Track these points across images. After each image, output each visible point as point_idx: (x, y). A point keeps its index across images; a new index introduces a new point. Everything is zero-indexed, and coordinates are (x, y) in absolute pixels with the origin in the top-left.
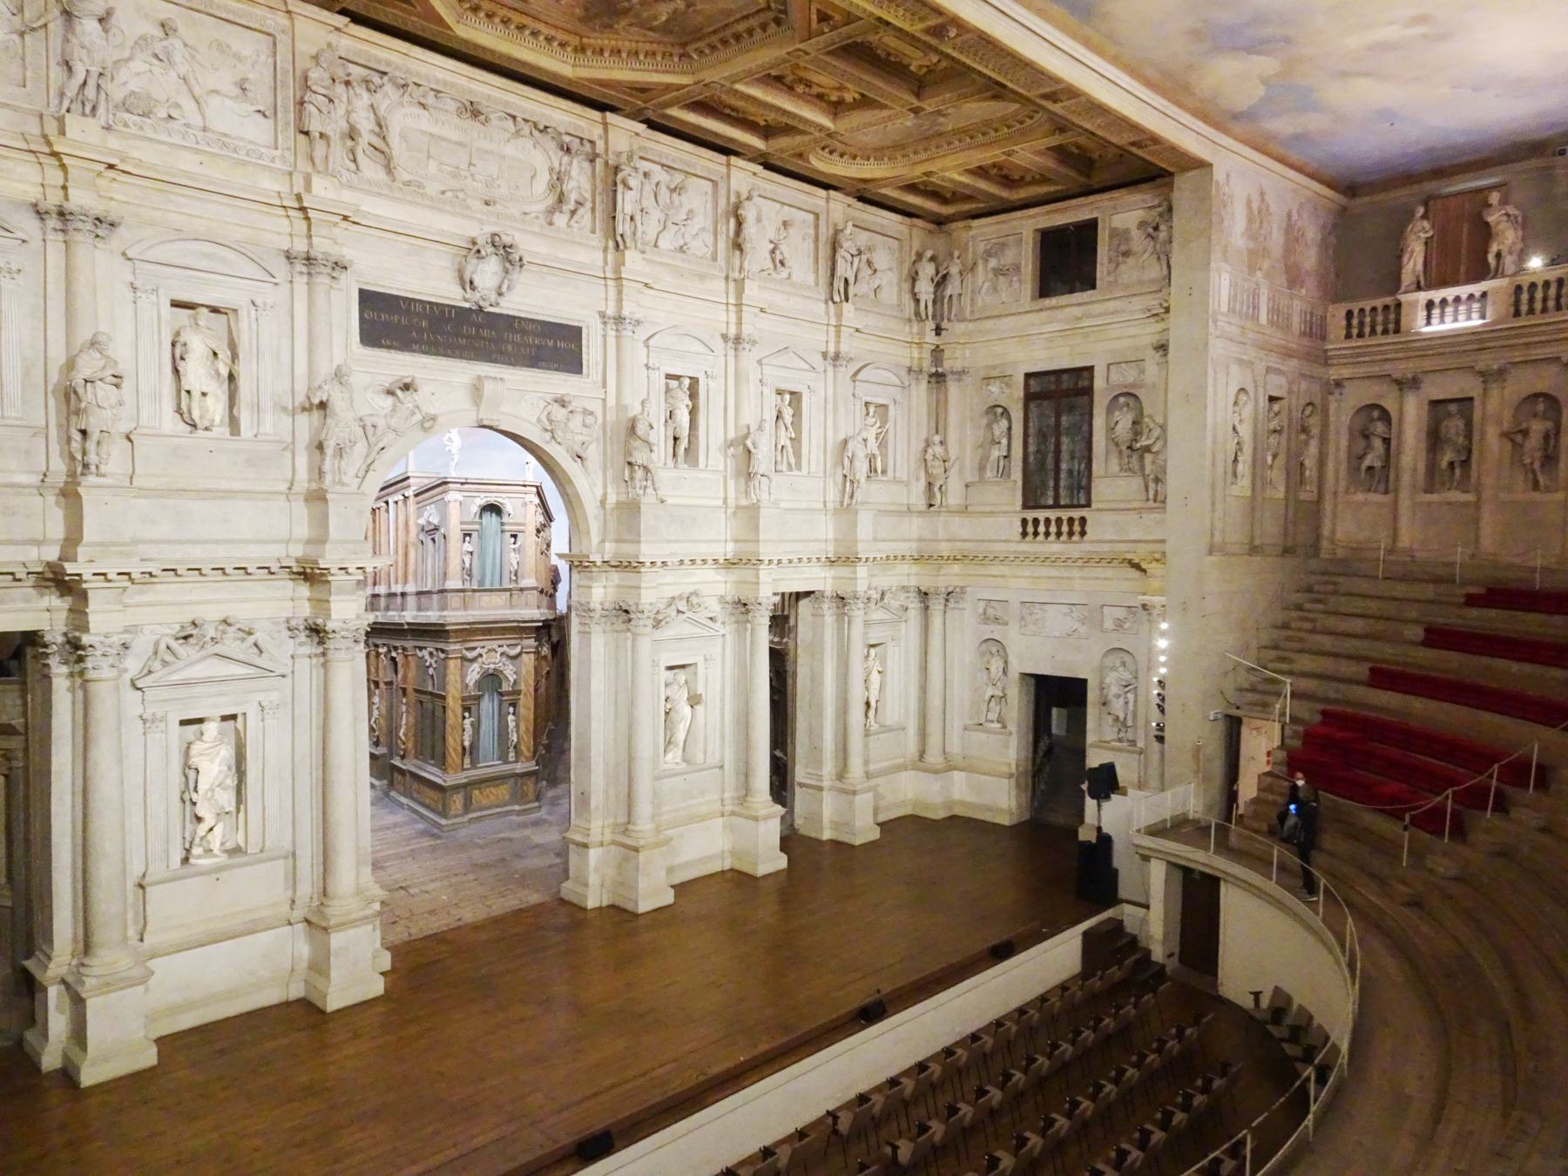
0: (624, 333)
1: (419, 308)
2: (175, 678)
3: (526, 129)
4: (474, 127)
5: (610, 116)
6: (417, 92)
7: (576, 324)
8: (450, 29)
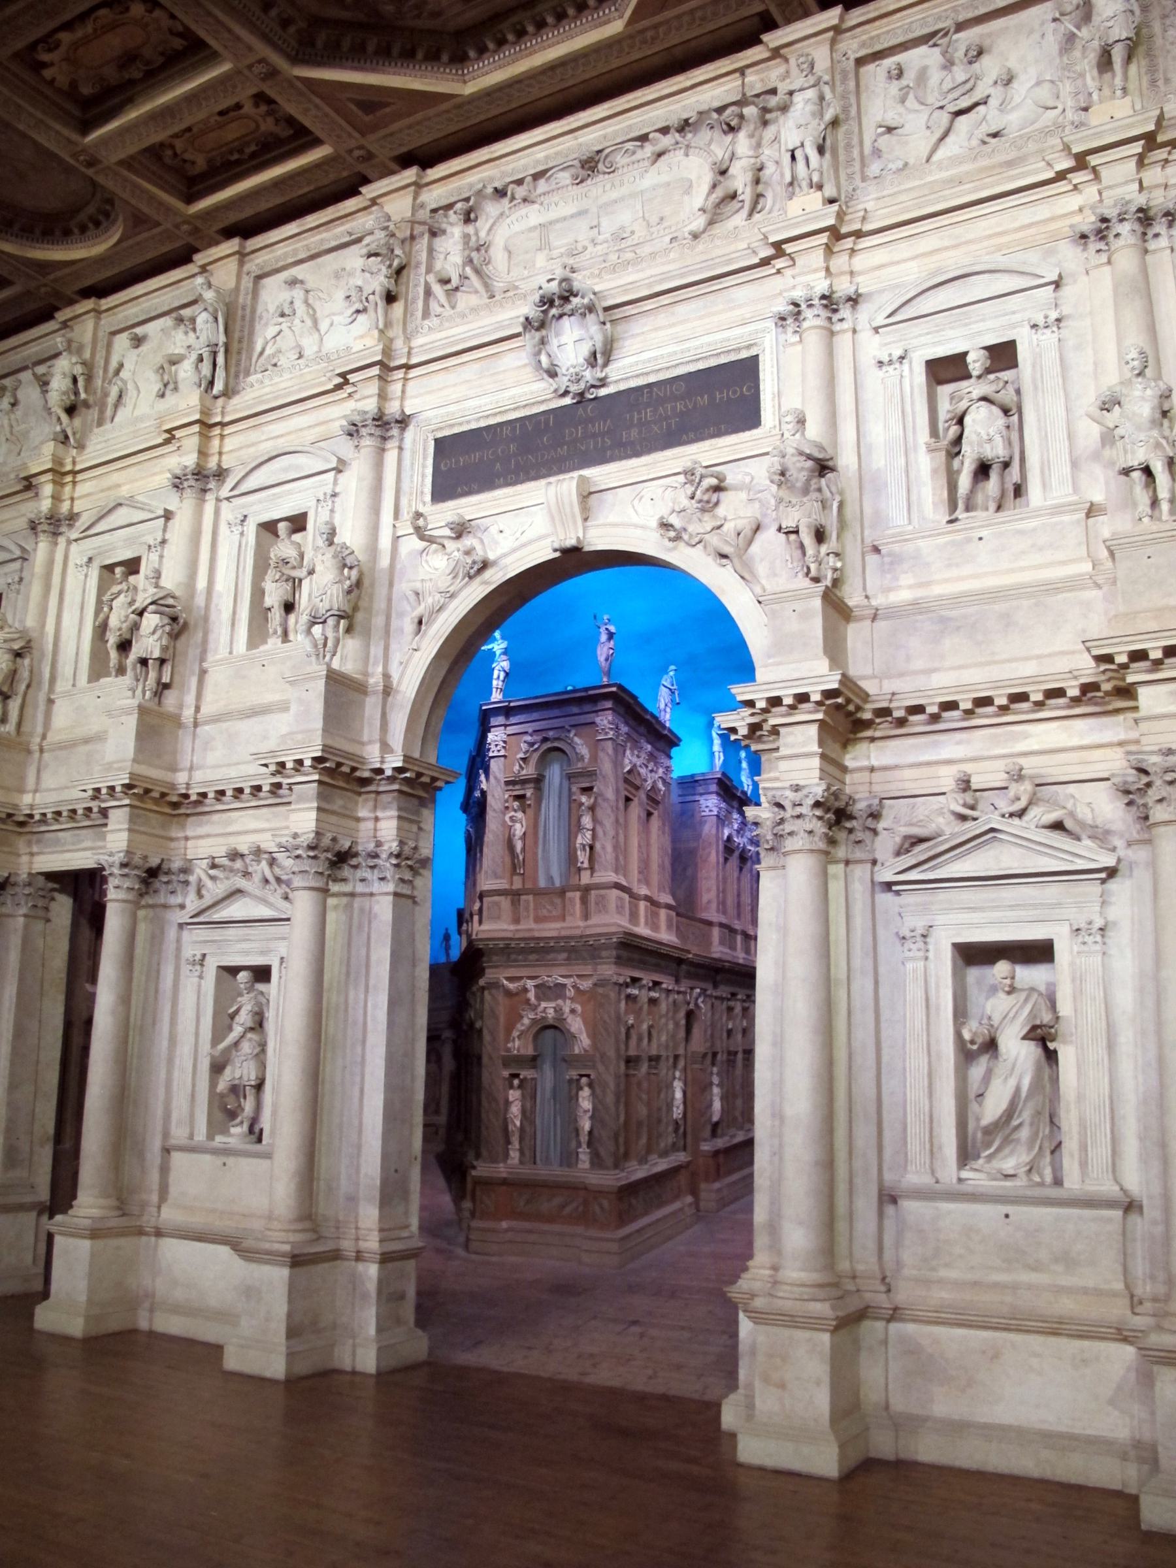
0: (805, 325)
1: (506, 431)
2: (217, 916)
3: (666, 141)
4: (599, 188)
5: (773, 39)
6: (520, 192)
7: (744, 354)
8: (457, 96)
